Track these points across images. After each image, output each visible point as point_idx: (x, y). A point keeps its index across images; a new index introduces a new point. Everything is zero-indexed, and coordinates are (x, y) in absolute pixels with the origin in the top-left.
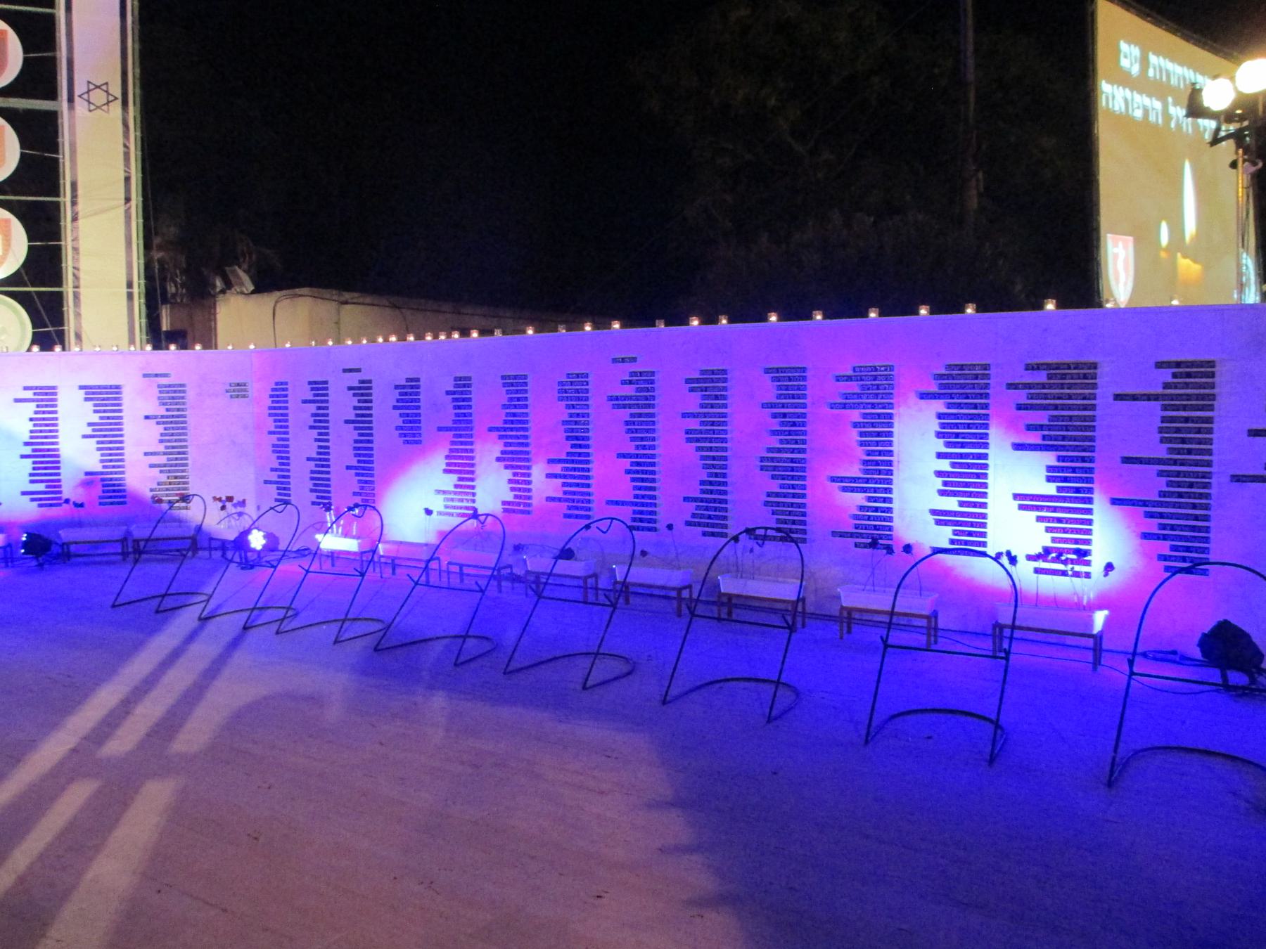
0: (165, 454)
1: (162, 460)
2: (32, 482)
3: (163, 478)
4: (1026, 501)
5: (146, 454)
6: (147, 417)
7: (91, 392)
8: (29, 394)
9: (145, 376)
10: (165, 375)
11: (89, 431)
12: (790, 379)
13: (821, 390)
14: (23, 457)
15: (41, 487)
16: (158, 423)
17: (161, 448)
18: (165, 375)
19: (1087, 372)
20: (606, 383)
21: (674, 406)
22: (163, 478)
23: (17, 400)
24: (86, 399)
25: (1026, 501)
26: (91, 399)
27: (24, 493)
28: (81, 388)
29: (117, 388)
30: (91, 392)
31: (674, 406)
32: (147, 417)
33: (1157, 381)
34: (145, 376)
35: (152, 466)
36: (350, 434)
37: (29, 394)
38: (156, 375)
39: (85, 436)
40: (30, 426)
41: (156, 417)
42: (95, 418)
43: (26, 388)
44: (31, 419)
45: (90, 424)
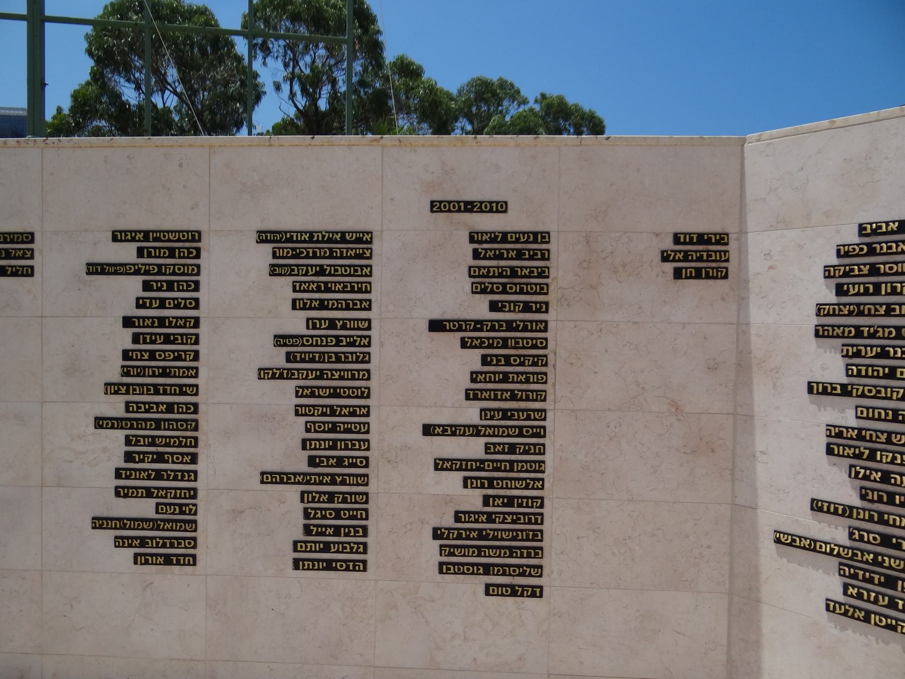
0: (476, 431)
1: (473, 448)
2: (119, 492)
3: (473, 500)
5: (428, 430)
6: (436, 326)
7: (291, 250)
8: (127, 253)
9: (437, 207)
10: (500, 207)
11: (277, 358)
14: (101, 423)
15: (145, 508)
16: (464, 344)
17: (471, 414)
18: (500, 207)
22: (473, 500)
23: (96, 269)
24: (274, 271)
26: (290, 271)
27: (99, 523)
28: (264, 237)
29: (359, 243)
30: (291, 250)
32: (436, 326)
34: (437, 207)
35: (441, 465)
37: (127, 253)
38: (469, 207)
39: (265, 373)
40: (125, 339)
41: (459, 325)
42: (296, 323)
43: (117, 237)
44: (128, 322)
45: (281, 340)
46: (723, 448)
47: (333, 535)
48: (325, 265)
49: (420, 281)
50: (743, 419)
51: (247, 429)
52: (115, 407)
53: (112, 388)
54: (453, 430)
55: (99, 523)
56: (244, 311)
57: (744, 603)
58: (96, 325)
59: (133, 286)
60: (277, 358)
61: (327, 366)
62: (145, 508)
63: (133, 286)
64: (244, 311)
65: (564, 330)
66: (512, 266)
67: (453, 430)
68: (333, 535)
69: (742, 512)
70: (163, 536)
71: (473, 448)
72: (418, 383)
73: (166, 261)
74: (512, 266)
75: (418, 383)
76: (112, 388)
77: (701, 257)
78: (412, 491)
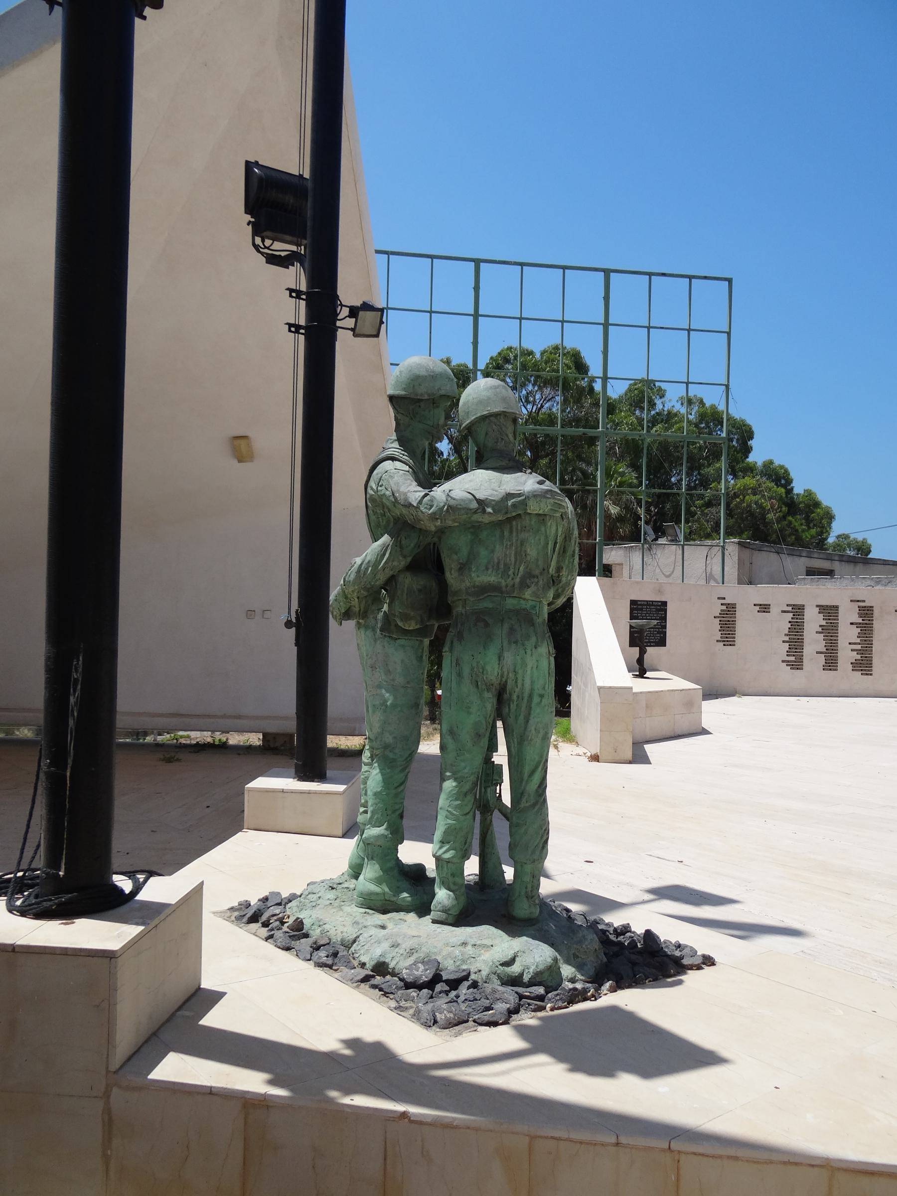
1: (859, 647)
3: (859, 657)
6: (852, 624)
8: (790, 609)
10: (864, 601)
11: (820, 629)
14: (784, 642)
15: (793, 658)
17: (858, 640)
18: (864, 601)
22: (859, 657)
27: (783, 661)
28: (817, 606)
32: (852, 624)
37: (790, 609)
40: (789, 625)
41: (856, 624)
42: (824, 623)
45: (820, 626)
47: (831, 663)
48: (829, 612)
49: (848, 615)
51: (813, 642)
52: (787, 639)
53: (786, 635)
54: (855, 644)
55: (783, 661)
56: (813, 620)
58: (784, 623)
59: (791, 615)
60: (820, 629)
61: (830, 631)
62: (793, 658)
63: (791, 615)
64: (813, 620)
65: (876, 624)
66: (866, 612)
67: (855, 644)
68: (831, 663)
70: (796, 664)
71: (859, 647)
72: (848, 634)
73: (798, 611)
74: (866, 612)
75: (848, 634)
76: (786, 635)
78: (846, 655)
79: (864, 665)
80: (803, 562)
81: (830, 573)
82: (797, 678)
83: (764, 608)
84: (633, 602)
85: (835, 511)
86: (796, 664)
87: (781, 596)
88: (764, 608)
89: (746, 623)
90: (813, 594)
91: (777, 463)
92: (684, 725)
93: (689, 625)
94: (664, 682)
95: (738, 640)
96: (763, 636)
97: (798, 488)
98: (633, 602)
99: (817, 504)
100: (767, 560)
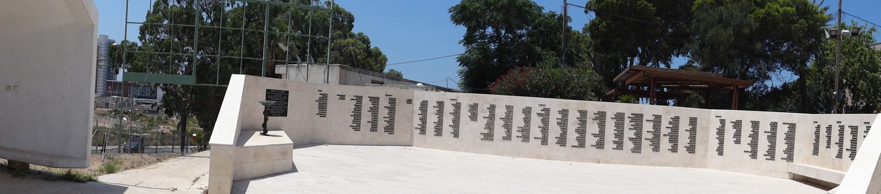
4: (631, 139)
12: (583, 113)
13: (590, 116)
19: (642, 116)
20: (536, 109)
21: (554, 117)
25: (631, 139)
31: (554, 117)
33: (652, 118)
36: (452, 117)
46: (410, 120)
47: (374, 128)
48: (375, 100)
49: (384, 103)
50: (413, 117)
51: (366, 116)
56: (366, 104)
57: (412, 134)
61: (374, 111)
64: (366, 104)
66: (393, 101)
68: (374, 128)
69: (412, 126)
70: (357, 128)
72: (383, 113)
73: (359, 99)
74: (393, 101)
75: (383, 113)
77: (409, 101)
78: (382, 123)
79: (390, 129)
80: (370, 78)
81: (382, 83)
82: (357, 136)
83: (342, 97)
84: (268, 91)
85: (388, 57)
86: (357, 128)
87: (351, 91)
88: (342, 97)
89: (332, 104)
90: (368, 91)
91: (365, 34)
92: (280, 166)
93: (300, 105)
94: (282, 138)
95: (328, 114)
96: (340, 113)
97: (372, 46)
98: (268, 91)
99: (380, 53)
100: (354, 75)
